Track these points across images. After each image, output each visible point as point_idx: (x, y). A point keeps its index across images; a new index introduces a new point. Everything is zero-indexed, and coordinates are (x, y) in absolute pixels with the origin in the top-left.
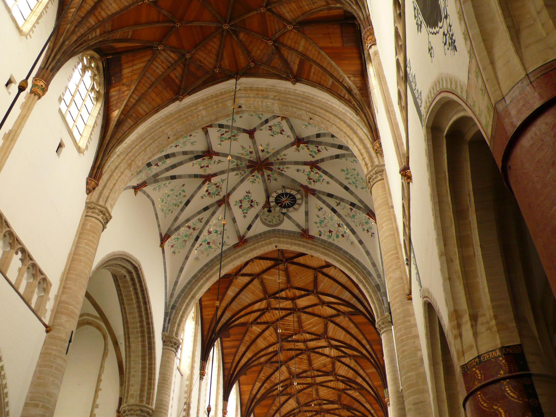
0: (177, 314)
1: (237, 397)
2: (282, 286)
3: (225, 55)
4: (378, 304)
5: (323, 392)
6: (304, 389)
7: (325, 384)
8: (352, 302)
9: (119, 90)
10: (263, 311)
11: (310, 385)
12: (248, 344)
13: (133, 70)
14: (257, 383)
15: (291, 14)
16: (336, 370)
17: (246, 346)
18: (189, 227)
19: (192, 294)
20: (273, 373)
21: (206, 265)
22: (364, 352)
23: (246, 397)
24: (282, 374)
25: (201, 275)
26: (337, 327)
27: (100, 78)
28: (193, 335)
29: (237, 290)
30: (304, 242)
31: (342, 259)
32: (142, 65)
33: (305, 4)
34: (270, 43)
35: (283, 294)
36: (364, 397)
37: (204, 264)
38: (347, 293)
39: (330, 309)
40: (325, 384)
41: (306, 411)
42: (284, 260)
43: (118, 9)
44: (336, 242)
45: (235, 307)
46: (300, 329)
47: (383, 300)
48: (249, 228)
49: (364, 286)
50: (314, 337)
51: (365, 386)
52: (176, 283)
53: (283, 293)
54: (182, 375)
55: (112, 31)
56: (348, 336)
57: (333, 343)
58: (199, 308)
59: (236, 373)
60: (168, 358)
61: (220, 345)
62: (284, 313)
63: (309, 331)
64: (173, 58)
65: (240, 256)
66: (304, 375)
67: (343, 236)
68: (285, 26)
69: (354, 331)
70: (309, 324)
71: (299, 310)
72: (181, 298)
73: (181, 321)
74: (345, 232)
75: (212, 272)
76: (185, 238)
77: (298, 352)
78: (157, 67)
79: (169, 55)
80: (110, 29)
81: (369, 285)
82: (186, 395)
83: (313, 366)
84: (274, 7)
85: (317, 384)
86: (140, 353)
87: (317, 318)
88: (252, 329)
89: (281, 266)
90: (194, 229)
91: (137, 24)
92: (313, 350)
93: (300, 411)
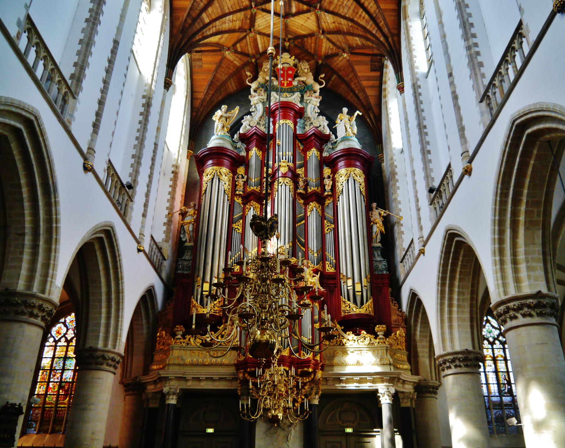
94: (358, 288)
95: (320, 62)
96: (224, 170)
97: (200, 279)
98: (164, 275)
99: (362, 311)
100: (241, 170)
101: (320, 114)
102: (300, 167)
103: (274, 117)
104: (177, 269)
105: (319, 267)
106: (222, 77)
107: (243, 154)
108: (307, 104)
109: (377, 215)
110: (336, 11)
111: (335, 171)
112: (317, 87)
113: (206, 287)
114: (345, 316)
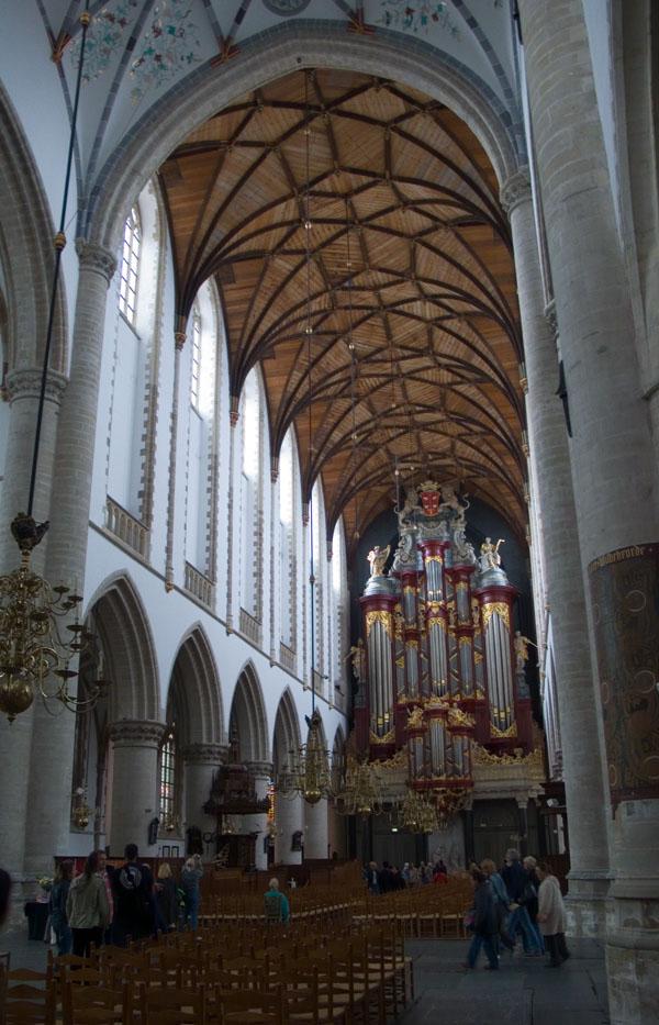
0: (104, 204)
1: (260, 398)
2: (323, 167)
4: (505, 152)
5: (416, 391)
6: (382, 385)
7: (417, 375)
8: (458, 191)
10: (294, 226)
11: (391, 378)
12: (270, 294)
14: (295, 372)
16: (436, 345)
17: (267, 297)
18: (111, 18)
19: (132, 163)
20: (323, 354)
21: (156, 105)
22: (484, 299)
23: (277, 398)
24: (338, 357)
25: (148, 126)
26: (433, 254)
28: (156, 265)
29: (237, 178)
30: (353, 41)
31: (433, 68)
35: (326, 185)
36: (486, 396)
37: (153, 102)
38: (451, 171)
39: (418, 216)
40: (417, 375)
41: (387, 427)
42: (322, 106)
44: (421, 35)
45: (234, 213)
46: (366, 263)
47: (515, 142)
48: (239, 17)
49: (479, 121)
50: (392, 278)
51: (486, 371)
52: (98, 141)
53: (326, 182)
54: (139, 339)
56: (455, 271)
57: (431, 289)
58: (165, 217)
59: (251, 348)
60: (92, 286)
61: (218, 298)
62: (334, 229)
63: (383, 266)
65: (225, 84)
66: (379, 356)
67: (435, 17)
69: (465, 259)
70: (381, 252)
71: (361, 222)
72: (110, 173)
73: (113, 217)
74: (440, 7)
75: (169, 119)
76: (105, 43)
77: (366, 312)
81: (488, 116)
82: (148, 372)
83: (394, 339)
85: (404, 375)
86: (30, 274)
87: (396, 238)
88: (276, 265)
89: (318, 122)
90: (122, 23)
92: (392, 308)
93: (376, 427)
94: (502, 715)
95: (463, 481)
96: (384, 613)
97: (374, 717)
98: (345, 710)
99: (506, 735)
100: (398, 608)
101: (466, 541)
102: (450, 600)
103: (424, 552)
104: (353, 705)
105: (470, 697)
106: (369, 504)
107: (398, 591)
108: (453, 531)
109: (522, 642)
110: (470, 457)
111: (481, 604)
112: (462, 511)
113: (380, 721)
114: (492, 740)
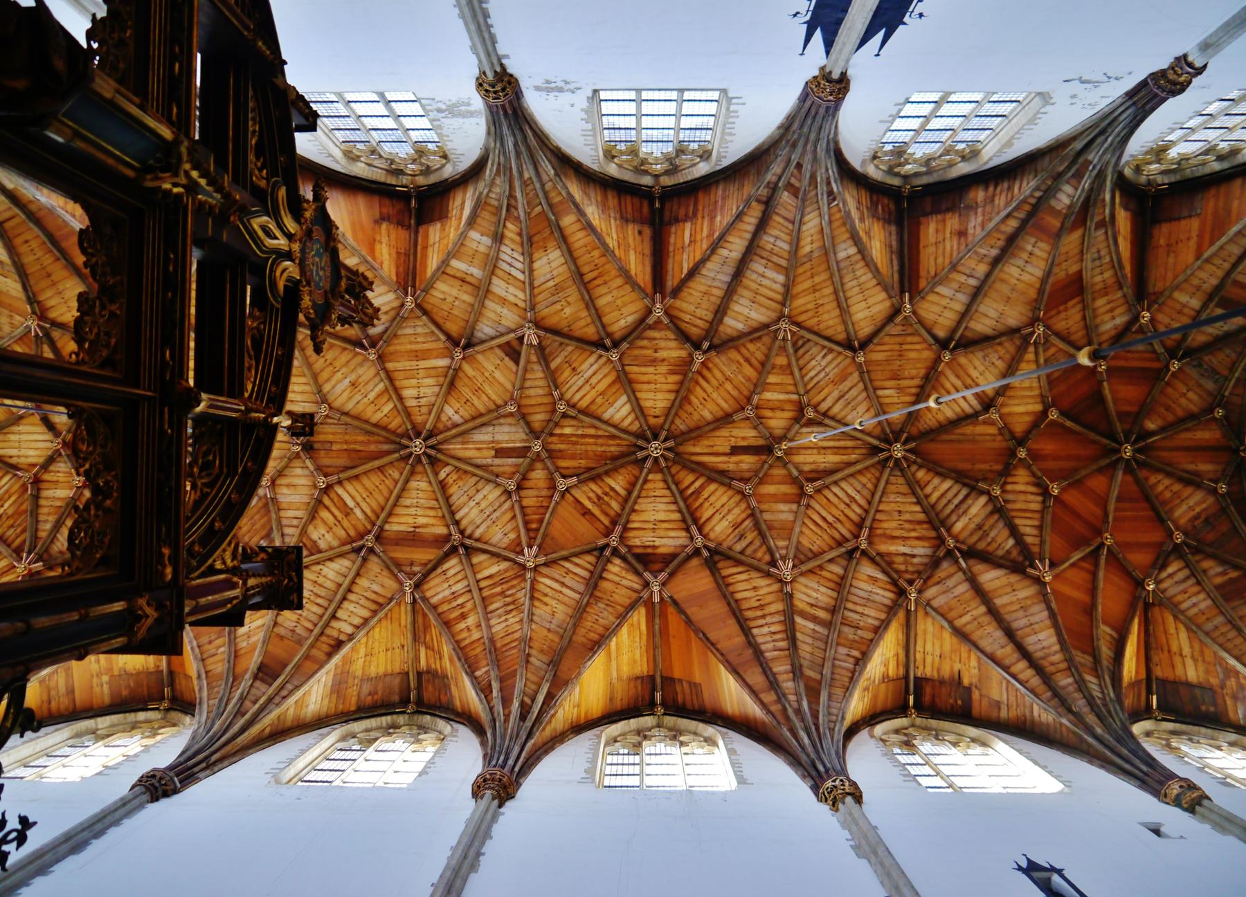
3: (1192, 467)
9: (1235, 698)
13: (1193, 657)
15: (1117, 312)
27: (1198, 734)
32: (1183, 634)
33: (1098, 279)
34: (1175, 365)
43: (1052, 631)
55: (1094, 657)
64: (1180, 570)
68: (1141, 330)
78: (1194, 605)
79: (1170, 576)
80: (1091, 659)
84: (1099, 335)
91: (1090, 610)
